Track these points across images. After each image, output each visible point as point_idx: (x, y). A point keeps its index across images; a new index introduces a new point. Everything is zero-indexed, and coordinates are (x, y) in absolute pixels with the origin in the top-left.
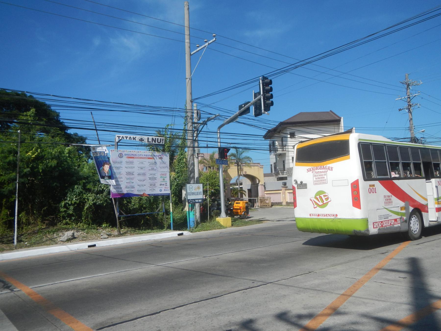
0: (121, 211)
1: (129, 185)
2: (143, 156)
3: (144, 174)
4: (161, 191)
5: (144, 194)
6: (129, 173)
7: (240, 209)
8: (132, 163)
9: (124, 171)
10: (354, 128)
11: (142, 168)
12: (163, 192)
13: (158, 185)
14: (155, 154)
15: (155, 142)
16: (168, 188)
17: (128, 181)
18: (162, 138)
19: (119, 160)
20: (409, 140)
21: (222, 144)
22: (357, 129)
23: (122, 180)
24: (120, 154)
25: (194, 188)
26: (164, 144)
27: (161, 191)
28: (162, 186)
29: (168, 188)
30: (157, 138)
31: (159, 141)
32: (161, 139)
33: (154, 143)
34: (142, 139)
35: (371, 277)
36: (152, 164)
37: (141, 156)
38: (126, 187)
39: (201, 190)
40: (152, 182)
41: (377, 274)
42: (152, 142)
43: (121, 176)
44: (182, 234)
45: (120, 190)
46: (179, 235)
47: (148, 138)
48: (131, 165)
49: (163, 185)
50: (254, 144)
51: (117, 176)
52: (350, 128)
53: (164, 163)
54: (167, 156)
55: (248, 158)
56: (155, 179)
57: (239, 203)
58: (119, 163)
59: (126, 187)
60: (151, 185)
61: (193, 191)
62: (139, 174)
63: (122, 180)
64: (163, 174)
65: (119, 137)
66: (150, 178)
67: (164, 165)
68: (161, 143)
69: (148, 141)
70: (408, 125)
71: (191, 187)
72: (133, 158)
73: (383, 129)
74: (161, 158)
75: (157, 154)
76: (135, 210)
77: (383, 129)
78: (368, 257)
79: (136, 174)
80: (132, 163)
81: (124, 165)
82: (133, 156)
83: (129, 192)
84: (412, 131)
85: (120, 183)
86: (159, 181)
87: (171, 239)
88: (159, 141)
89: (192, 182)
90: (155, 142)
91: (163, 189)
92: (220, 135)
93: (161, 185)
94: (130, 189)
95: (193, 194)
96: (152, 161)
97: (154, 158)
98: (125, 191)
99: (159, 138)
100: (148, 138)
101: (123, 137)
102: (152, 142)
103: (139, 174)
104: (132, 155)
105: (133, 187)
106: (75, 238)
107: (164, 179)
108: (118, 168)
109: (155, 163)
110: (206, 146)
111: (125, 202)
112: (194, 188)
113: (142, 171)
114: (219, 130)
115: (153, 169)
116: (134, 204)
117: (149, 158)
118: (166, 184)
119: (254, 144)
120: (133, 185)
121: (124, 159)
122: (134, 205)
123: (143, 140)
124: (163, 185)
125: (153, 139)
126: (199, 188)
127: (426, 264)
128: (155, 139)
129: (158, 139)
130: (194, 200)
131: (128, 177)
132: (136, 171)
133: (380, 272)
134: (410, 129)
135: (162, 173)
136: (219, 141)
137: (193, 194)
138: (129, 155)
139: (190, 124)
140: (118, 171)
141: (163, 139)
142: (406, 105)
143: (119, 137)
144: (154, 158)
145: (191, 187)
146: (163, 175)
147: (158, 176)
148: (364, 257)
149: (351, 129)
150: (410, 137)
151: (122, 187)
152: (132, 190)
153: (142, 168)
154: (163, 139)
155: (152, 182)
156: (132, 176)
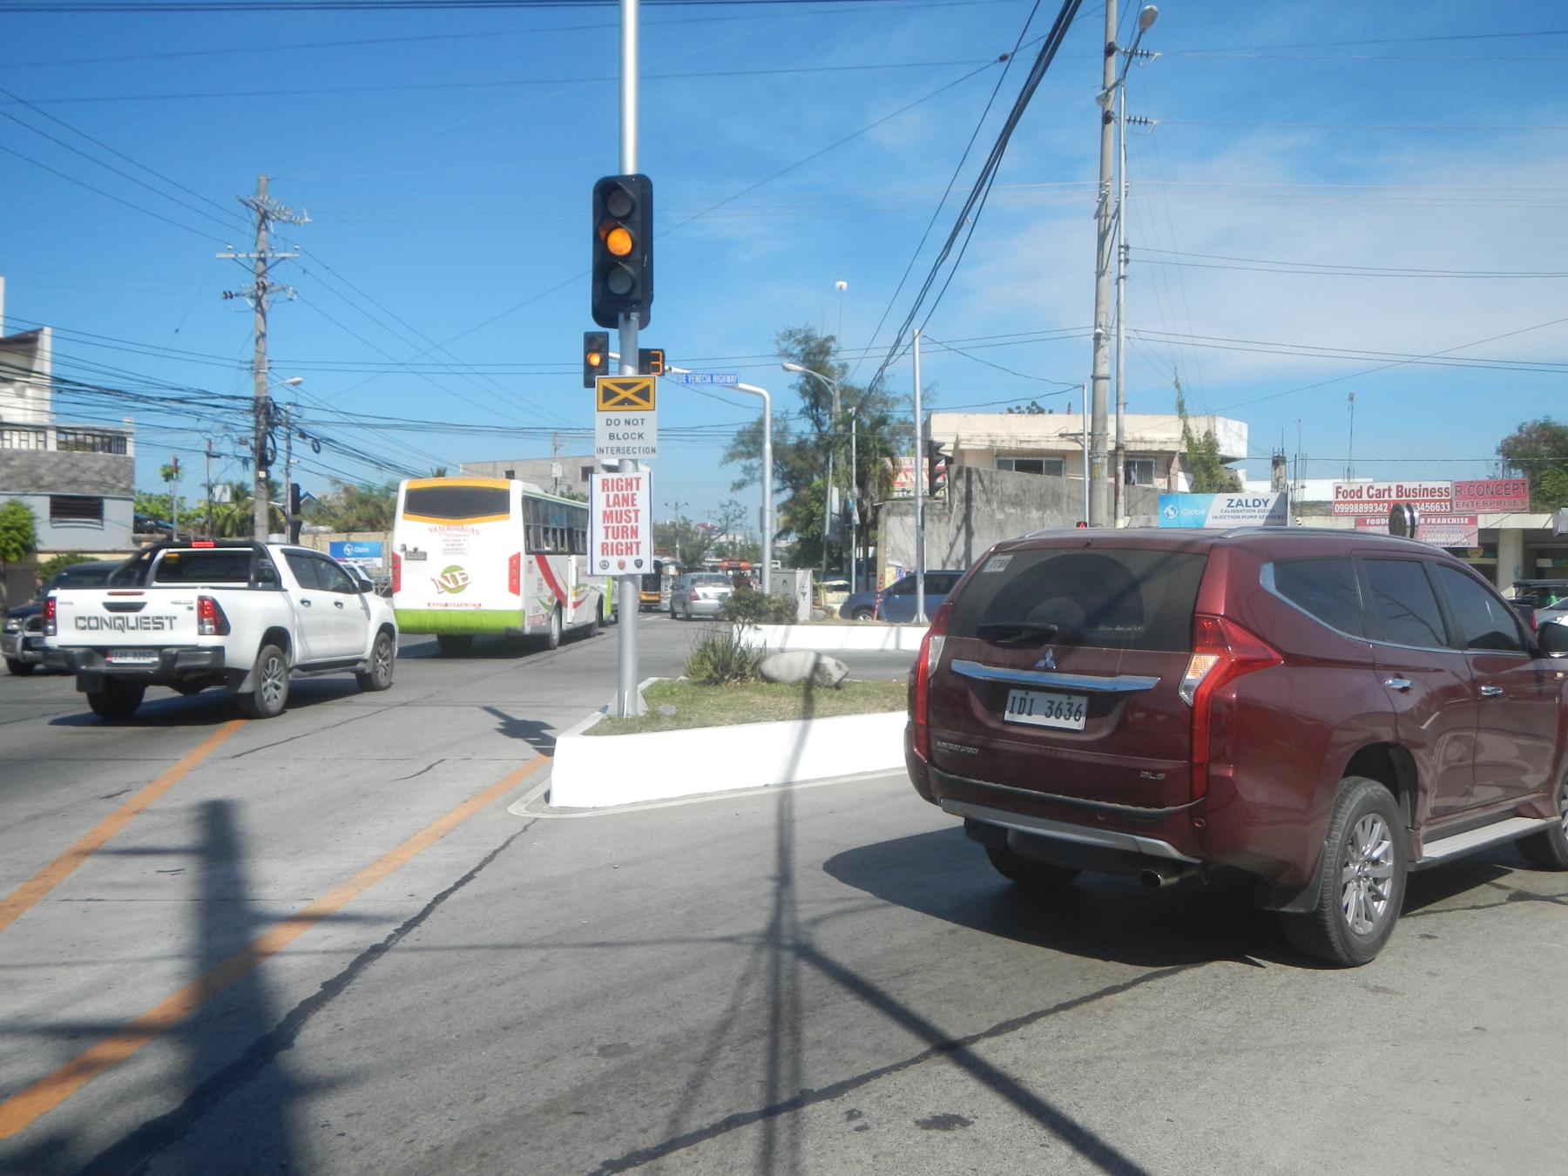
10: (47, 330)
20: (248, 405)
22: (61, 333)
35: (50, 888)
41: (77, 871)
52: (31, 328)
70: (249, 354)
73: (161, 352)
77: (161, 352)
78: (51, 814)
84: (261, 378)
127: (255, 819)
133: (89, 863)
134: (255, 368)
142: (249, 284)
148: (35, 818)
149: (37, 332)
150: (252, 394)
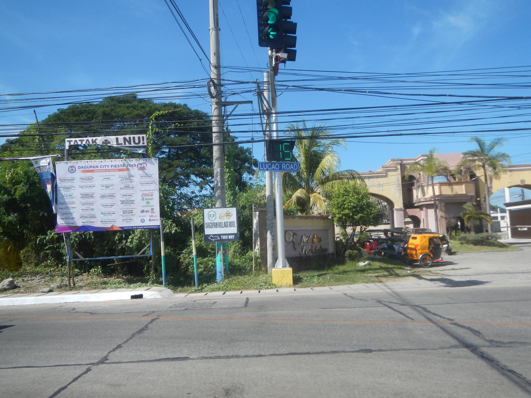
0: (76, 253)
1: (86, 213)
2: (110, 168)
3: (112, 196)
4: (143, 221)
5: (112, 226)
6: (85, 196)
7: (415, 249)
8: (90, 179)
9: (77, 192)
11: (107, 187)
12: (147, 223)
13: (137, 211)
14: (131, 163)
15: (130, 143)
16: (156, 216)
17: (84, 207)
18: (141, 136)
19: (70, 176)
21: (281, 134)
23: (74, 205)
24: (71, 167)
25: (218, 216)
26: (146, 144)
27: (143, 221)
28: (144, 214)
29: (156, 216)
30: (132, 136)
31: (137, 141)
32: (139, 138)
33: (127, 144)
34: (106, 140)
36: (127, 179)
37: (107, 168)
38: (82, 217)
39: (234, 218)
40: (126, 207)
42: (125, 143)
43: (72, 200)
44: (141, 296)
45: (71, 221)
46: (133, 297)
47: (117, 139)
48: (88, 183)
49: (147, 211)
50: (353, 126)
51: (67, 200)
53: (147, 175)
54: (153, 164)
55: (503, 155)
56: (132, 202)
57: (415, 238)
58: (69, 180)
59: (82, 217)
60: (125, 212)
61: (218, 220)
62: (103, 197)
63: (74, 205)
64: (146, 195)
65: (70, 142)
66: (123, 202)
67: (147, 180)
68: (141, 144)
69: (118, 144)
71: (212, 213)
72: (92, 171)
74: (143, 169)
75: (134, 161)
76: (131, 250)
79: (97, 196)
80: (90, 179)
81: (77, 183)
82: (92, 169)
83: (86, 224)
85: (71, 211)
86: (139, 204)
87: (119, 304)
88: (137, 141)
89: (218, 204)
90: (130, 143)
91: (147, 219)
92: (276, 117)
93: (143, 211)
94: (88, 220)
95: (216, 225)
96: (126, 173)
97: (128, 170)
98: (80, 223)
99: (136, 136)
100: (117, 139)
101: (76, 141)
102: (125, 143)
103: (103, 197)
104: (91, 167)
105: (93, 217)
106: (16, 287)
107: (148, 203)
108: (67, 188)
109: (131, 176)
110: (250, 139)
111: (117, 238)
112: (218, 216)
113: (108, 192)
114: (275, 109)
115: (127, 187)
116: (132, 242)
117: (120, 170)
118: (153, 209)
119: (353, 126)
120: (93, 213)
121: (78, 174)
122: (131, 242)
123: (109, 142)
124: (147, 211)
125: (125, 139)
126: (228, 215)
128: (130, 138)
129: (134, 138)
130: (220, 235)
131: (84, 201)
132: (98, 191)
135: (145, 192)
136: (274, 129)
137: (216, 225)
138: (85, 167)
139: (214, 106)
140: (68, 193)
141: (143, 137)
143: (70, 142)
144: (128, 170)
145: (212, 213)
146: (146, 196)
147: (137, 197)
151: (74, 216)
152: (92, 220)
153: (107, 187)
154: (143, 137)
155: (126, 207)
156: (91, 200)
